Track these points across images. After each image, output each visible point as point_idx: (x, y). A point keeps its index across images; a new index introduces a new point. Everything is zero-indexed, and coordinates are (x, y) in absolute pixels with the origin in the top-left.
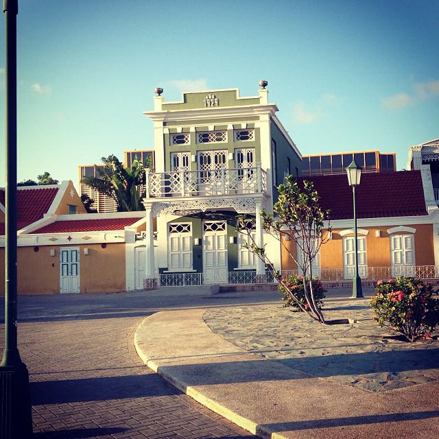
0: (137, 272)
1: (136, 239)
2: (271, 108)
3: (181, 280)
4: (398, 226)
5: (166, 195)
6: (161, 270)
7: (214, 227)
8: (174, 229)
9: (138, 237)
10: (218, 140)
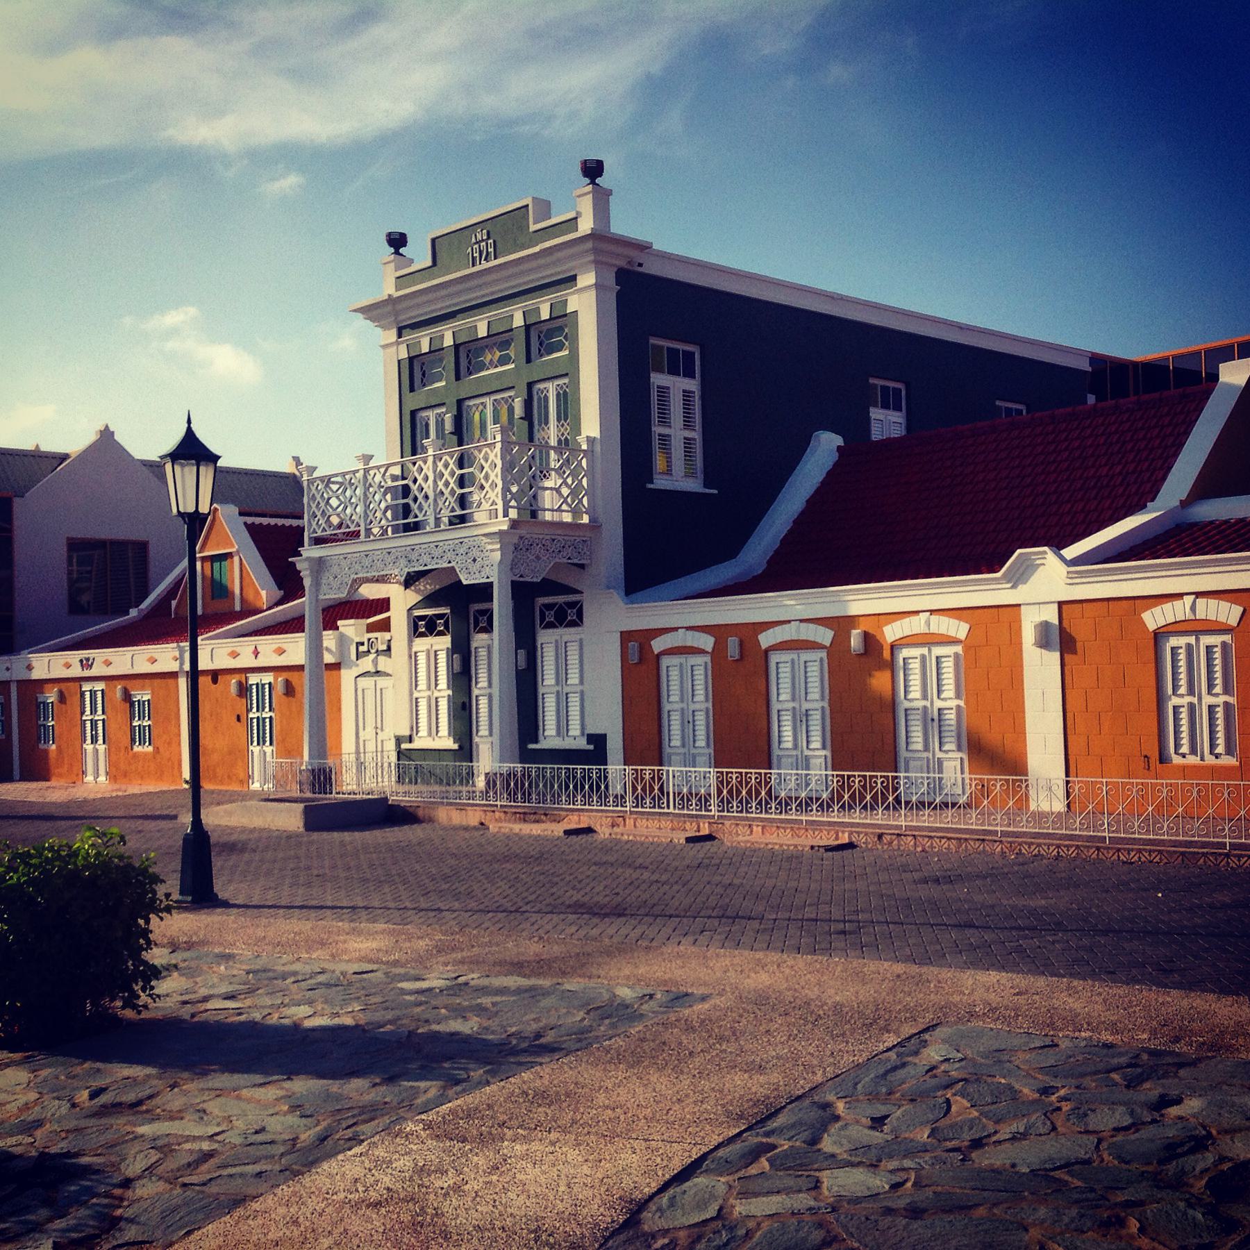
2: (589, 245)
5: (408, 528)
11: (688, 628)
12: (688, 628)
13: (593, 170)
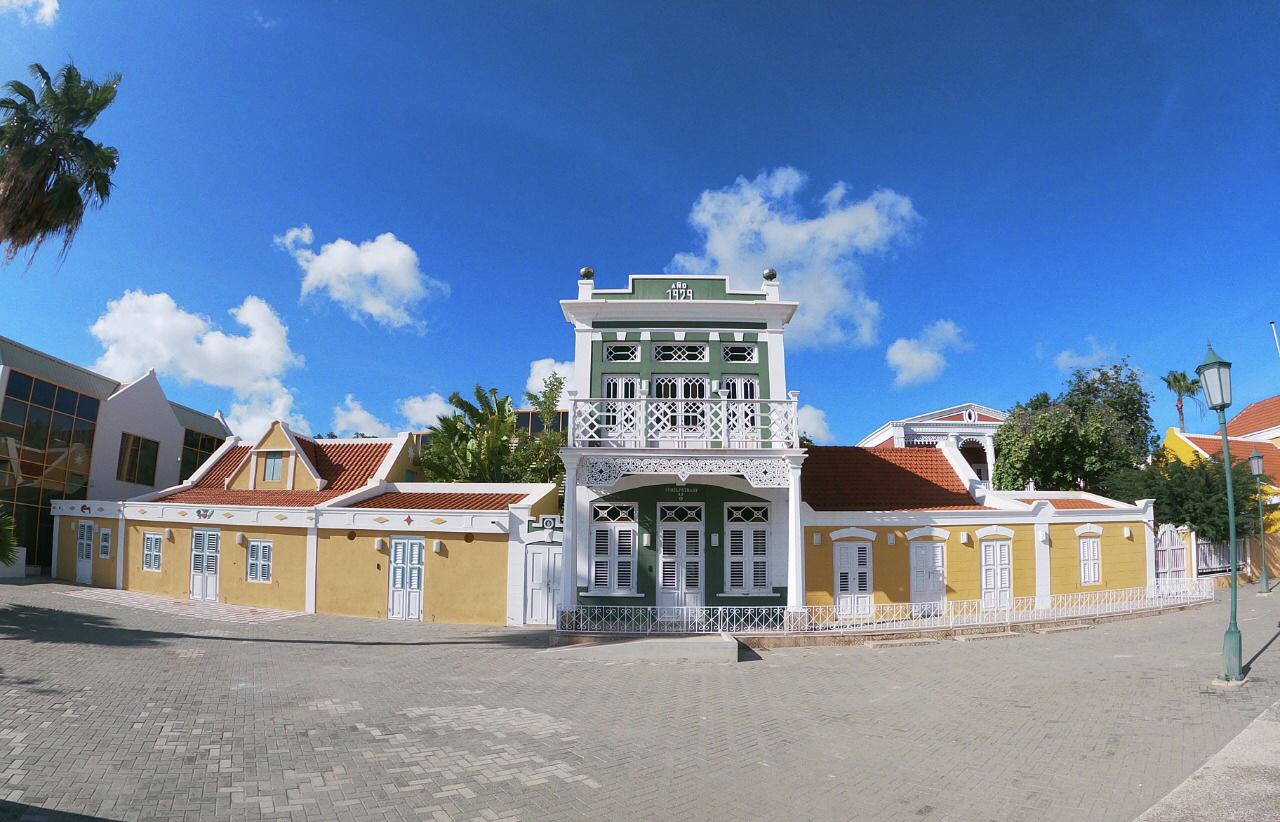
7: (681, 515)
8: (603, 513)
9: (534, 525)
11: (857, 527)
12: (857, 527)
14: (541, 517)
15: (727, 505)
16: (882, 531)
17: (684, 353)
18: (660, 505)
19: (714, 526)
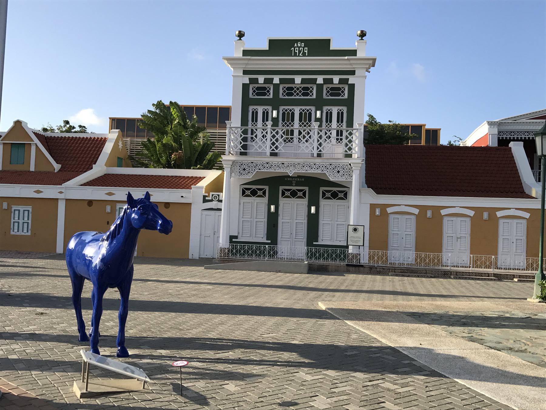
0: (203, 237)
1: (205, 201)
3: (264, 252)
4: (510, 209)
6: (231, 237)
7: (294, 194)
9: (207, 198)
10: (304, 94)
11: (406, 205)
12: (406, 205)
13: (363, 35)
14: (211, 193)
15: (322, 189)
16: (423, 209)
17: (300, 92)
18: (281, 188)
19: (314, 201)
